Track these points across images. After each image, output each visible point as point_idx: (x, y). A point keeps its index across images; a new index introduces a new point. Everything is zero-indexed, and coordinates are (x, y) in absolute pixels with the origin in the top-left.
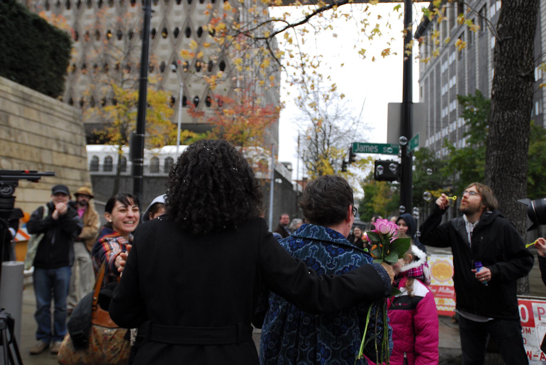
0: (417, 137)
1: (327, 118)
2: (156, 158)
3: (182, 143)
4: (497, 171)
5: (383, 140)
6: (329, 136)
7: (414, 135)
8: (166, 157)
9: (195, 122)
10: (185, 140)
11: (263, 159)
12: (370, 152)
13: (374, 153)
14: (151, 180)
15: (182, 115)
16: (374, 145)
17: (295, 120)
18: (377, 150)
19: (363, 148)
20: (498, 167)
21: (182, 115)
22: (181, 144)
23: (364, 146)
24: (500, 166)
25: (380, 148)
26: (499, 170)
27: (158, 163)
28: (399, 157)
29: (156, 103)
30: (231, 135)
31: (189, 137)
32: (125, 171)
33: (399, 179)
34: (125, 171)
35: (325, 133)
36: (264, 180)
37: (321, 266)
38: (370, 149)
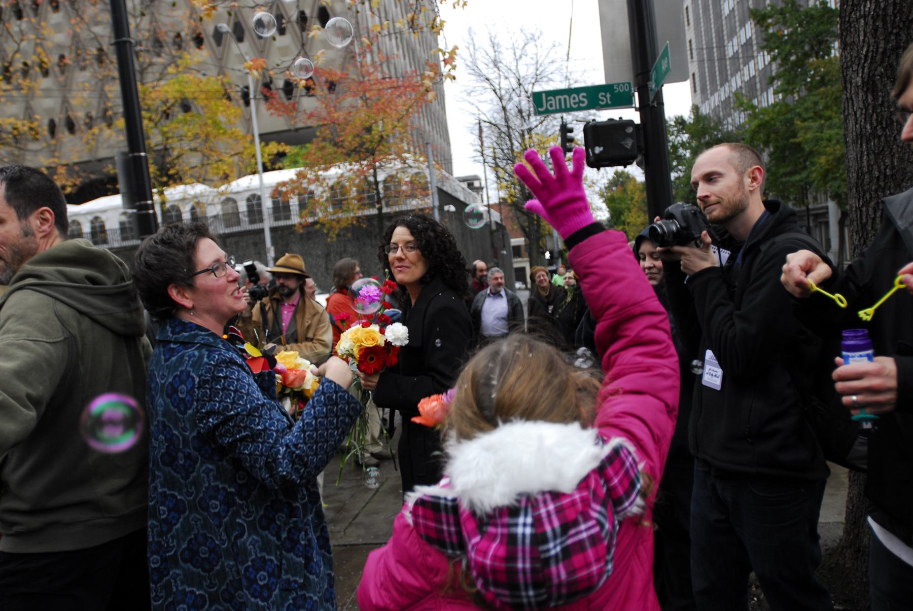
1: (520, 85)
2: (230, 201)
3: (268, 165)
4: (878, 57)
5: (597, 77)
6: (529, 115)
7: (661, 51)
8: (247, 195)
9: (292, 128)
10: (273, 162)
11: (417, 174)
13: (580, 109)
14: (228, 241)
15: (264, 118)
16: (578, 91)
17: (464, 95)
18: (585, 100)
19: (554, 101)
20: (882, 45)
21: (264, 118)
22: (266, 169)
23: (557, 98)
24: (887, 41)
25: (593, 97)
26: (884, 53)
27: (237, 208)
28: (636, 110)
30: (350, 138)
31: (281, 155)
33: (640, 158)
37: (179, 497)
38: (571, 102)
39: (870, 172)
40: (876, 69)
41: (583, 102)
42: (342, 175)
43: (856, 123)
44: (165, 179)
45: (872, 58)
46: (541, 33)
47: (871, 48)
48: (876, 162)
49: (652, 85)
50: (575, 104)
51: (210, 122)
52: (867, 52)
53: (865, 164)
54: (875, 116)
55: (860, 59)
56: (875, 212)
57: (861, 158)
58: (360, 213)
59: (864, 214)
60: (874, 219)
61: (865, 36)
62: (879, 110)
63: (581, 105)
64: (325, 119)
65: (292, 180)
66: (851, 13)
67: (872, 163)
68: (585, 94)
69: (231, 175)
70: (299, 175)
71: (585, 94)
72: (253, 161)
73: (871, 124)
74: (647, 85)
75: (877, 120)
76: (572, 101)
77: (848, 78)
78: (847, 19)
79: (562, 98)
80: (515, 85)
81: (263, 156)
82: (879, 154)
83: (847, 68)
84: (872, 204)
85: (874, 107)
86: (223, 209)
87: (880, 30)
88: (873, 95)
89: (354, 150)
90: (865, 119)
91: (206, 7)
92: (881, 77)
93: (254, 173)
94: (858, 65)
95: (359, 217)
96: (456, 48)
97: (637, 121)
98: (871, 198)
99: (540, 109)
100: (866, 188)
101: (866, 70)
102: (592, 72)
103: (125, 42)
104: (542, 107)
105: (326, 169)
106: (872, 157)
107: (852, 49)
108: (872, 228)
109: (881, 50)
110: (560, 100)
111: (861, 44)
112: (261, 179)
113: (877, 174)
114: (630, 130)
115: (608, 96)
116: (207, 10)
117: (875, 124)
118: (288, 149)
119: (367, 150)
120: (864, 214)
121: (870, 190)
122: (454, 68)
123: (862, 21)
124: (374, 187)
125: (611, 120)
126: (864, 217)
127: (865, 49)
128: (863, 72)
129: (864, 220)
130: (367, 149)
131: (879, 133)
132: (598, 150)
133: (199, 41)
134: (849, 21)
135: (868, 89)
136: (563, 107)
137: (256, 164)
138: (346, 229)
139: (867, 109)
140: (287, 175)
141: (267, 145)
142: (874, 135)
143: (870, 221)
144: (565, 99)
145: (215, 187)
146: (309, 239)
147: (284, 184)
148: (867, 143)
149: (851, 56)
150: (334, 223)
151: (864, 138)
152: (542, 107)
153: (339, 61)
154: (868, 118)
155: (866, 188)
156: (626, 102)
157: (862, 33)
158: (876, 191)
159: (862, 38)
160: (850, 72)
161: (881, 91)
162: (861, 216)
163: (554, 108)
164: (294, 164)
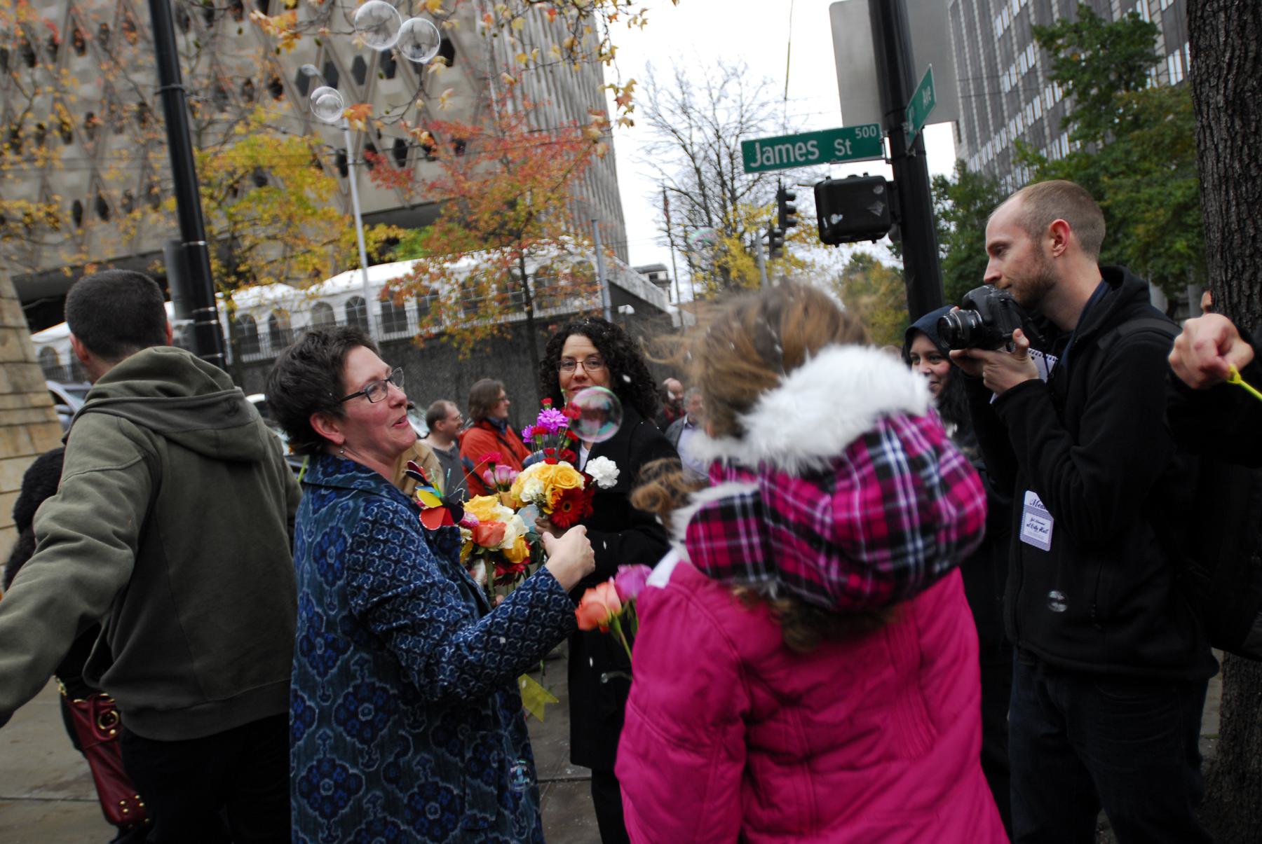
0: (928, 81)
1: (719, 137)
2: (323, 307)
3: (375, 255)
4: (1248, 66)
5: (830, 117)
6: (733, 179)
7: (919, 79)
8: (347, 297)
9: (406, 205)
10: (382, 252)
11: (580, 263)
12: (797, 164)
15: (368, 193)
17: (642, 153)
18: (816, 150)
21: (368, 193)
22: (371, 262)
23: (777, 148)
25: (826, 145)
27: (333, 316)
28: (887, 162)
29: (289, 166)
30: (486, 216)
31: (392, 242)
32: (257, 350)
33: (894, 228)
34: (257, 350)
35: (720, 174)
36: (587, 313)
38: (796, 152)
39: (1242, 230)
40: (1245, 83)
41: (813, 153)
42: (476, 268)
43: (1218, 161)
44: (233, 279)
45: (1239, 67)
46: (746, 67)
47: (1237, 53)
48: (1250, 215)
49: (909, 127)
50: (801, 155)
51: (293, 198)
52: (1231, 58)
53: (1234, 218)
54: (1246, 149)
55: (1221, 69)
56: (1251, 288)
57: (1228, 210)
58: (502, 320)
59: (1235, 290)
60: (1250, 297)
61: (1227, 36)
62: (1252, 141)
63: (810, 157)
64: (452, 191)
65: (407, 276)
66: (1204, 5)
67: (1244, 216)
68: (815, 142)
69: (324, 270)
70: (419, 269)
71: (815, 142)
72: (354, 251)
73: (1241, 161)
74: (901, 129)
75: (1249, 155)
76: (797, 152)
77: (1203, 98)
78: (1199, 14)
79: (783, 148)
80: (712, 138)
81: (367, 244)
82: (1253, 203)
83: (1201, 83)
84: (1247, 275)
85: (1244, 136)
86: (313, 318)
87: (1249, 27)
88: (1242, 120)
89: (493, 233)
90: (1232, 154)
91: (284, 34)
92: (1254, 94)
93: (355, 268)
94: (1219, 77)
95: (501, 325)
96: (633, 82)
97: (889, 177)
98: (1244, 266)
99: (753, 165)
100: (1236, 252)
101: (1230, 84)
102: (823, 111)
103: (175, 90)
104: (755, 161)
105: (454, 260)
106: (1244, 208)
107: (1207, 57)
108: (1248, 309)
109: (1251, 55)
110: (780, 151)
111: (1222, 47)
112: (365, 276)
113: (1252, 232)
114: (879, 190)
115: (848, 143)
116: (286, 38)
117: (1247, 161)
118: (401, 234)
119: (511, 232)
120: (1235, 290)
121: (1241, 255)
122: (631, 109)
123: (1222, 15)
124: (521, 282)
125: (854, 176)
126: (1235, 295)
127: (1228, 55)
128: (1226, 87)
129: (1235, 300)
130: (510, 230)
131: (1254, 172)
132: (835, 219)
133: (277, 89)
134: (1202, 17)
135: (1234, 111)
136: (785, 161)
137: (358, 255)
138: (483, 341)
139: (1233, 140)
140: (401, 269)
141: (372, 228)
142: (1246, 176)
143: (1244, 301)
144: (787, 150)
145: (302, 288)
146: (432, 357)
147: (397, 281)
148: (1236, 189)
149: (1207, 66)
150: (468, 334)
151: (1231, 181)
152: (755, 161)
153: (469, 112)
154: (1235, 152)
155: (1236, 252)
156: (871, 151)
157: (1222, 33)
158: (1252, 256)
159: (1222, 39)
160: (1206, 89)
161: (1254, 113)
162: (1230, 293)
163: (772, 162)
164: (411, 254)
